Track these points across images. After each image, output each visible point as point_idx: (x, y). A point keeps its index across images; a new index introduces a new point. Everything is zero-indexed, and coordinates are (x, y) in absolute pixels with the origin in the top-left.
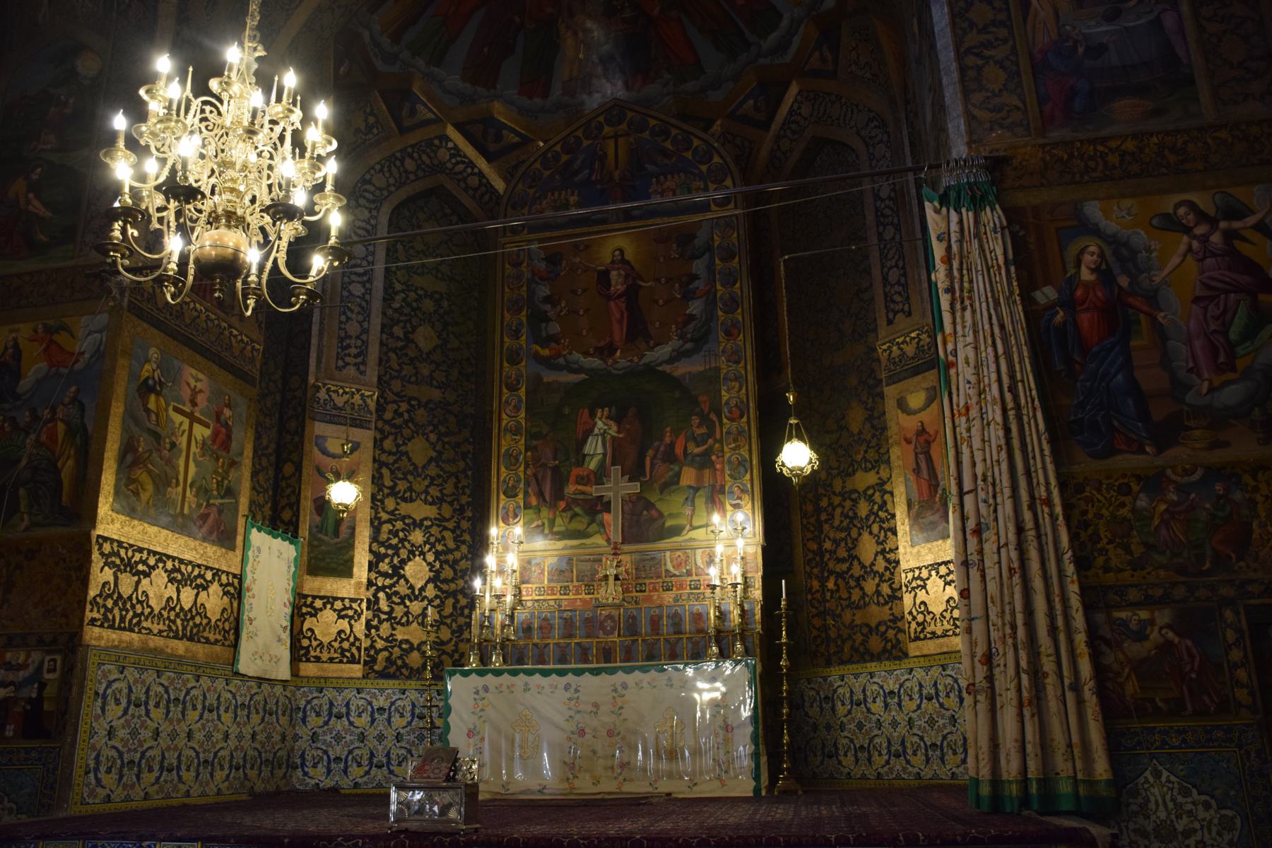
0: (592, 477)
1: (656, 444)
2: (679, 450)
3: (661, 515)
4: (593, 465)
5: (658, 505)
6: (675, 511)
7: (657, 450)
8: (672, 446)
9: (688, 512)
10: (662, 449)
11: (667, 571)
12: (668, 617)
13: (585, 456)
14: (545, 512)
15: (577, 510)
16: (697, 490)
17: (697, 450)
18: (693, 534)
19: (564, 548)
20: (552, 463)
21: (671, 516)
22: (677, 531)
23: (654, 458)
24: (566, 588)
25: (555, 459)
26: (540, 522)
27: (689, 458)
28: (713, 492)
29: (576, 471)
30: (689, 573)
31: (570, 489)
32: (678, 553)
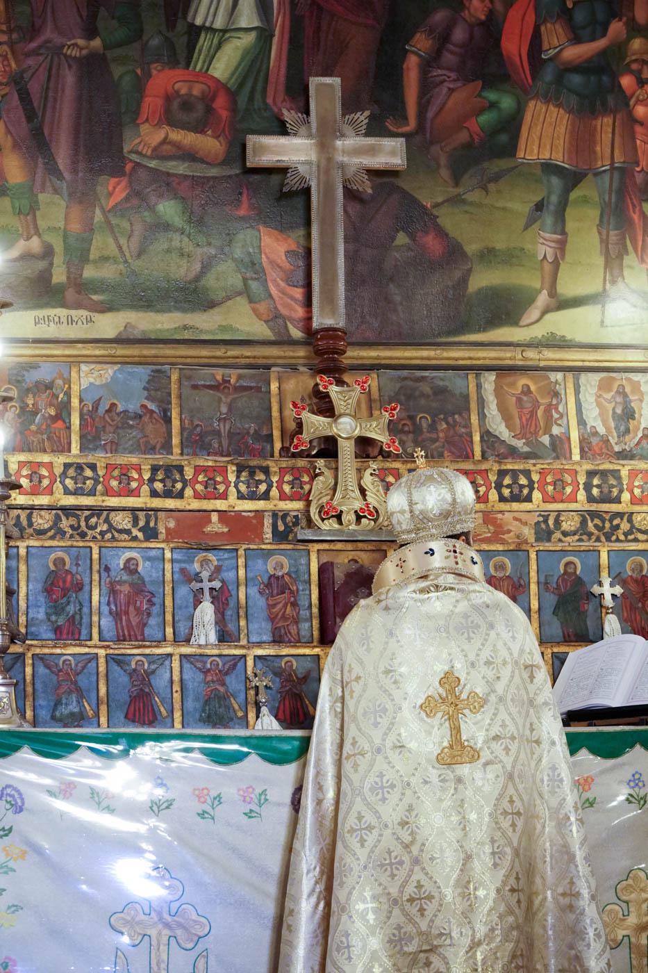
0: (220, 103)
1: (439, 16)
2: (513, 45)
3: (454, 253)
4: (224, 65)
5: (450, 220)
6: (500, 242)
7: (444, 39)
8: (491, 29)
9: (544, 248)
10: (459, 34)
11: (487, 436)
12: (544, 585)
13: (195, 32)
14: (55, 211)
15: (168, 209)
16: (573, 179)
17: (573, 53)
18: (565, 323)
19: (118, 341)
20: (79, 46)
21: (489, 256)
22: (504, 308)
23: (427, 65)
24: (172, 471)
25: (91, 33)
26: (35, 244)
27: (548, 74)
28: (622, 192)
29: (163, 80)
30: (559, 447)
31: (146, 137)
32: (523, 381)
